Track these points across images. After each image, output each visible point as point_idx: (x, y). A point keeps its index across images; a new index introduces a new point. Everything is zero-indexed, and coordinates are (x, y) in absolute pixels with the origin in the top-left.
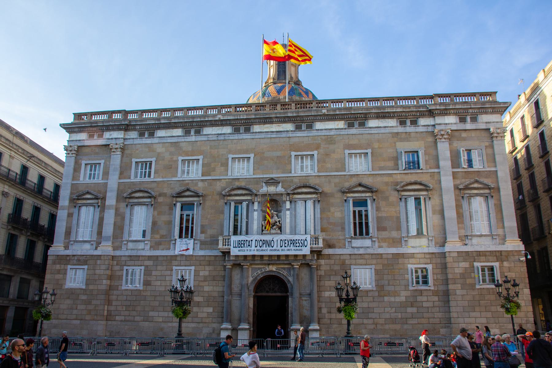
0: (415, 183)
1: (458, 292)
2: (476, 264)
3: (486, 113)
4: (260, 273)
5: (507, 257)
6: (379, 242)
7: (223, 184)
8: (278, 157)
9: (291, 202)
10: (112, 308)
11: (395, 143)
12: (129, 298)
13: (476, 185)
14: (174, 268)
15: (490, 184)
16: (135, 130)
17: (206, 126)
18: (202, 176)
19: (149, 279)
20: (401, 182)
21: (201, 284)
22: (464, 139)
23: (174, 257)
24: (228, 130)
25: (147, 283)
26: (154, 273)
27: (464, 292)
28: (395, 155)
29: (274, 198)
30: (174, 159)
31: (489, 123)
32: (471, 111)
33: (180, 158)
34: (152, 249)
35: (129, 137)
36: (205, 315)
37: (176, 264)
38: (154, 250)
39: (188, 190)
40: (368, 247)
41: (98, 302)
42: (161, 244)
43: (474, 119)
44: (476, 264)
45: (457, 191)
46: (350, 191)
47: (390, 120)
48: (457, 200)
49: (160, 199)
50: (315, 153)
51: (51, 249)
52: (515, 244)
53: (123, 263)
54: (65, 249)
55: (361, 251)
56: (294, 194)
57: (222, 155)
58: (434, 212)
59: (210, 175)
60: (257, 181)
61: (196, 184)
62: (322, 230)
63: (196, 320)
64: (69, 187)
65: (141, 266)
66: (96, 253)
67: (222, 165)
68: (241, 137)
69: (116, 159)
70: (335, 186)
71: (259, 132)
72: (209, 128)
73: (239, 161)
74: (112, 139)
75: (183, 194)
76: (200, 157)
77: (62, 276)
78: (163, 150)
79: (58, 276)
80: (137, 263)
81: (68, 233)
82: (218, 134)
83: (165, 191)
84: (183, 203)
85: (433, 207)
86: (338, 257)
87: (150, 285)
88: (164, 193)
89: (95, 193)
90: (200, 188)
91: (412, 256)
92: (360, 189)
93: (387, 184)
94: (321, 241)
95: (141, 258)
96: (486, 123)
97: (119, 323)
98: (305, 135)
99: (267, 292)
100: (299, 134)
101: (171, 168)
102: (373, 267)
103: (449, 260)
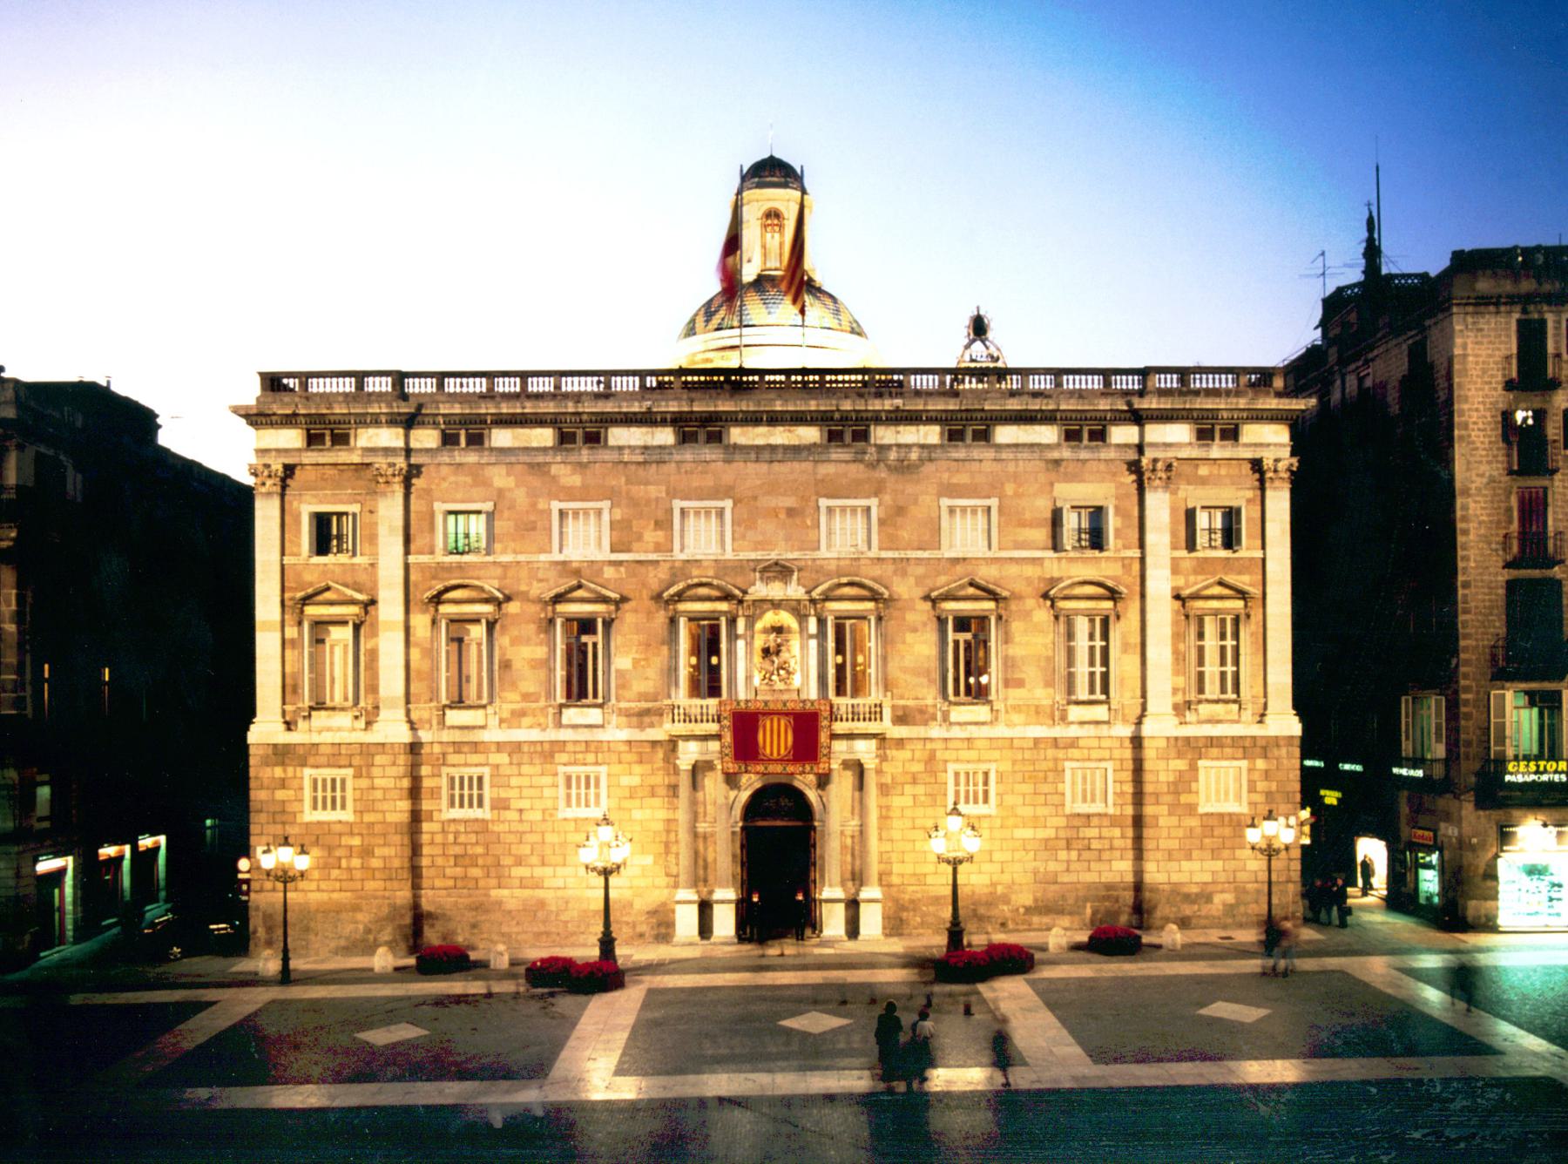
1: (1162, 822)
5: (1265, 748)
7: (663, 574)
11: (1052, 484)
12: (462, 839)
19: (503, 795)
20: (1060, 580)
22: (1203, 481)
26: (514, 781)
27: (1174, 820)
31: (1261, 445)
33: (556, 506)
39: (580, 586)
40: (983, 724)
41: (386, 851)
44: (1201, 763)
45: (1178, 604)
46: (950, 597)
48: (1175, 623)
50: (873, 502)
51: (252, 727)
57: (657, 499)
58: (1126, 648)
59: (629, 551)
60: (740, 567)
67: (658, 525)
70: (917, 584)
76: (605, 505)
77: (291, 792)
78: (510, 482)
79: (280, 795)
81: (288, 689)
85: (1124, 636)
87: (507, 808)
91: (1073, 743)
92: (971, 591)
93: (1029, 580)
96: (1256, 445)
100: (837, 454)
101: (534, 529)
103: (1149, 753)
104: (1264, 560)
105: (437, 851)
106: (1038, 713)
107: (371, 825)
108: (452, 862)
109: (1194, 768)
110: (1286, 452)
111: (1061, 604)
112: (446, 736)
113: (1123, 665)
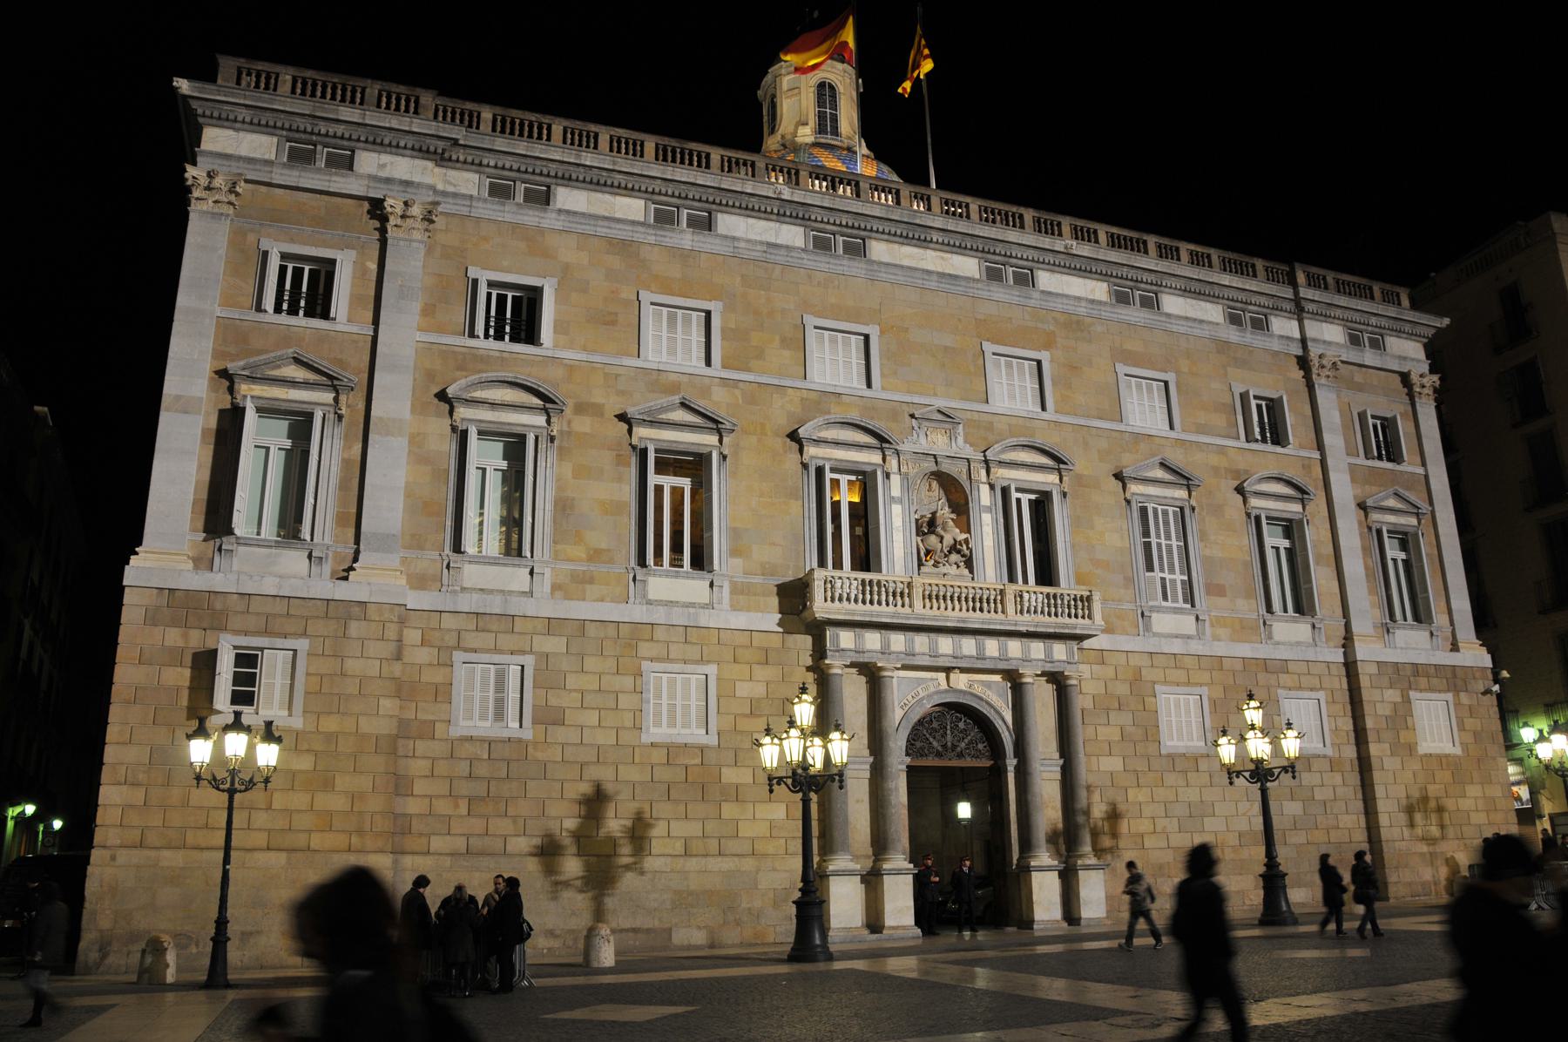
0: (1279, 479)
1: (1391, 763)
2: (1412, 693)
3: (1399, 333)
4: (922, 694)
6: (1212, 625)
8: (946, 348)
9: (992, 487)
10: (413, 806)
12: (482, 770)
13: (1392, 503)
14: (646, 665)
15: (1419, 503)
16: (478, 166)
17: (728, 208)
18: (724, 367)
19: (553, 701)
21: (744, 725)
22: (1360, 388)
23: (641, 632)
24: (793, 235)
25: (549, 718)
26: (572, 681)
28: (1227, 399)
29: (946, 467)
30: (624, 295)
31: (1405, 358)
32: (1373, 320)
34: (558, 594)
35: (451, 189)
36: (762, 829)
37: (653, 653)
38: (568, 597)
40: (1189, 637)
41: (364, 783)
42: (591, 581)
43: (1377, 345)
47: (1209, 306)
48: (1361, 534)
49: (583, 425)
50: (1044, 356)
52: (1476, 656)
53: (451, 640)
54: (196, 567)
55: (1176, 647)
56: (1001, 463)
59: (748, 370)
61: (706, 392)
62: (1080, 579)
63: (731, 846)
64: (210, 328)
65: (523, 652)
66: (342, 591)
68: (839, 269)
69: (410, 260)
71: (888, 264)
72: (734, 218)
73: (833, 341)
74: (388, 181)
75: (663, 416)
80: (506, 641)
82: (769, 245)
83: (598, 397)
84: (665, 446)
86: (1122, 659)
88: (594, 405)
89: (323, 364)
90: (718, 402)
91: (1283, 666)
92: (1160, 474)
93: (1216, 470)
94: (1097, 606)
95: (518, 624)
97: (448, 861)
98: (1016, 300)
99: (939, 755)
100: (998, 292)
101: (613, 323)
102: (1205, 691)
103: (1364, 681)
104: (1426, 477)
105: (441, 788)
106: (1242, 630)
107: (332, 737)
108: (464, 810)
109: (1407, 701)
110: (1425, 368)
111: (1254, 502)
112: (466, 603)
113: (1321, 579)
